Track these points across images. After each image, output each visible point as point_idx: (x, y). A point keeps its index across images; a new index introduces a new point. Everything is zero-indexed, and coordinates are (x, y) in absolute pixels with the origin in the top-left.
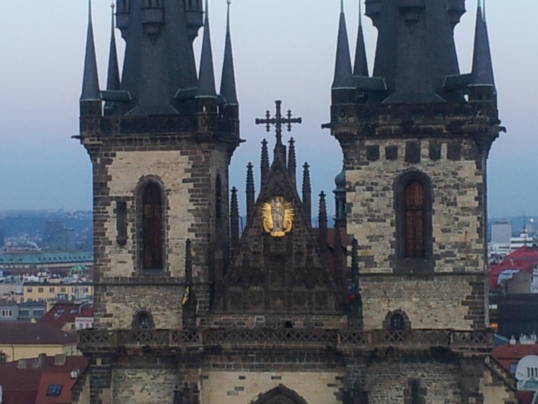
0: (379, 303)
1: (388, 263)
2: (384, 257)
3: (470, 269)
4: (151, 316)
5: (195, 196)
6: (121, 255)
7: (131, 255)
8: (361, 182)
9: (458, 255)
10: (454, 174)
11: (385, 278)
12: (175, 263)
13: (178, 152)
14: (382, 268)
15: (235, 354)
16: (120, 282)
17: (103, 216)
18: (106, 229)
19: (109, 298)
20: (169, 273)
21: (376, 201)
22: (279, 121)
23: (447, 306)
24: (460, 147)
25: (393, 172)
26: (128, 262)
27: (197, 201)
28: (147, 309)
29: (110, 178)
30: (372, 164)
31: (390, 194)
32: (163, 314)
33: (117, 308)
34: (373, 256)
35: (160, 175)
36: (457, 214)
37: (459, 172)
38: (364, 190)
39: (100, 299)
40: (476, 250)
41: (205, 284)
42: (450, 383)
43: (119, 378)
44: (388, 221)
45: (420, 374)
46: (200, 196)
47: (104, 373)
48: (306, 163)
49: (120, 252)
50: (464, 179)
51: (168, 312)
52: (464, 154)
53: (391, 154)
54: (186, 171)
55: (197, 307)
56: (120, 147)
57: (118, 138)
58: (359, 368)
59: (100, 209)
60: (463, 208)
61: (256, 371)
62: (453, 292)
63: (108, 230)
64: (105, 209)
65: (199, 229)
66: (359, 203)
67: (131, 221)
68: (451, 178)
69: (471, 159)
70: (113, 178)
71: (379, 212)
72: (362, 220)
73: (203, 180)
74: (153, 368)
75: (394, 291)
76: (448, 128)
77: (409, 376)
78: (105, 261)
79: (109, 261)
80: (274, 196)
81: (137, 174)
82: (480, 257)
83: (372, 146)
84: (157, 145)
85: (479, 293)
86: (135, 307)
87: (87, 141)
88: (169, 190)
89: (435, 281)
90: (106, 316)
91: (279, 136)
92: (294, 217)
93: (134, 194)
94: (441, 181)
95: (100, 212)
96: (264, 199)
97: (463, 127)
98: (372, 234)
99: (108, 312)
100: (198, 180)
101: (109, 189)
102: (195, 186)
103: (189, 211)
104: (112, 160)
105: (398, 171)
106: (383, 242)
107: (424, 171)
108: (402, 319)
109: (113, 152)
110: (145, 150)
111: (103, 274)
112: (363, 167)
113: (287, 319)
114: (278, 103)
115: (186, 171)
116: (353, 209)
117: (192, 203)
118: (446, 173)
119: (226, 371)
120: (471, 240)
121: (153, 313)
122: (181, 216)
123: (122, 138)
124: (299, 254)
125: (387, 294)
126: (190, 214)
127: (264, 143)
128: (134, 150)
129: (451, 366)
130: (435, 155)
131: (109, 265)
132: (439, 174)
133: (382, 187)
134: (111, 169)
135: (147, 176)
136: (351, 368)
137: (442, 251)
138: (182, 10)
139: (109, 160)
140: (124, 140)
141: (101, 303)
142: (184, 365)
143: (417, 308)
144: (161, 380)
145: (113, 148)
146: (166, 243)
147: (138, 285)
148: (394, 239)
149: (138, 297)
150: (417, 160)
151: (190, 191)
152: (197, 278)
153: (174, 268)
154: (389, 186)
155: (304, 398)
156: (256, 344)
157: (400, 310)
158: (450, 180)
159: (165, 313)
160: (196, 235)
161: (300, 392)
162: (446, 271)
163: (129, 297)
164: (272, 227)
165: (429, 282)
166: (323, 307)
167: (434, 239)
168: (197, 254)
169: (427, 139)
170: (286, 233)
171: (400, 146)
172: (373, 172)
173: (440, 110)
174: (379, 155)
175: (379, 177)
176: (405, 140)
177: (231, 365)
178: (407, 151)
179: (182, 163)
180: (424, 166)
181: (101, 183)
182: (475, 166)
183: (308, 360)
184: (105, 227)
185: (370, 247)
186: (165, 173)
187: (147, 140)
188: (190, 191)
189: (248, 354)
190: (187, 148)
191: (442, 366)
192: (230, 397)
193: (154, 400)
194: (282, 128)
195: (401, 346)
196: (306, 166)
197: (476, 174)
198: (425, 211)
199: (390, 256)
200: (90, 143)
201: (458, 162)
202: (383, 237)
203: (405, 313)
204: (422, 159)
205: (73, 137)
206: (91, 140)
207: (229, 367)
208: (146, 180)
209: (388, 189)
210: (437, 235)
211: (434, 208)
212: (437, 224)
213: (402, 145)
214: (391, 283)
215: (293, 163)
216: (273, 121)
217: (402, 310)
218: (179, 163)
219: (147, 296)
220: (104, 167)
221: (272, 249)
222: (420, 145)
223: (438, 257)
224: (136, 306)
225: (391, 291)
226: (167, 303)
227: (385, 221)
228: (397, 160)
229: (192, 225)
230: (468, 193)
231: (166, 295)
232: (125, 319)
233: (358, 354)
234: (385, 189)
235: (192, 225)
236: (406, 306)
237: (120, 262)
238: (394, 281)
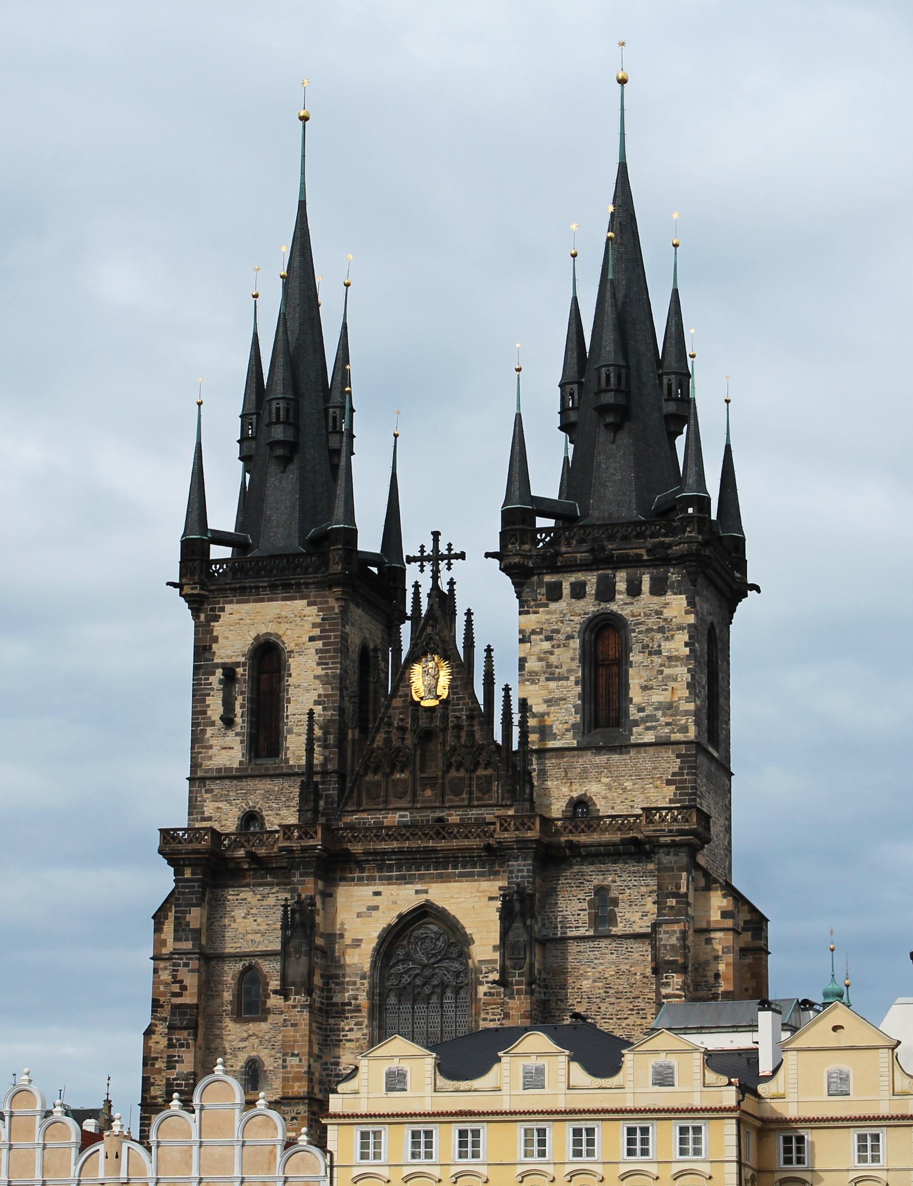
0: (557, 787)
1: (571, 734)
2: (566, 726)
3: (678, 737)
4: (262, 818)
5: (325, 658)
9: (662, 719)
10: (659, 613)
11: (567, 753)
12: (295, 746)
13: (305, 602)
15: (368, 861)
16: (225, 775)
18: (209, 706)
19: (209, 795)
20: (287, 760)
21: (556, 653)
22: (436, 558)
23: (647, 786)
24: (667, 578)
25: (580, 615)
27: (327, 664)
28: (257, 809)
29: (215, 640)
30: (553, 606)
31: (576, 643)
34: (551, 726)
35: (280, 633)
36: (661, 665)
37: (665, 611)
38: (541, 640)
39: (196, 797)
40: (686, 711)
41: (333, 772)
42: (649, 889)
43: (216, 900)
44: (572, 678)
45: (610, 879)
46: (330, 658)
47: (193, 887)
48: (469, 610)
49: (225, 735)
50: (671, 620)
51: (284, 812)
52: (672, 587)
53: (578, 592)
55: (322, 803)
57: (228, 586)
58: (524, 866)
59: (201, 679)
60: (670, 658)
61: (396, 884)
62: (655, 769)
64: (208, 679)
65: (328, 700)
66: (535, 658)
68: (653, 619)
69: (681, 594)
72: (538, 680)
73: (335, 637)
74: (260, 885)
75: (579, 770)
76: (649, 552)
77: (596, 882)
79: (211, 747)
80: (425, 655)
82: (690, 720)
85: (690, 768)
87: (187, 590)
88: (292, 652)
89: (632, 754)
90: (204, 819)
91: (435, 577)
92: (452, 680)
94: (641, 623)
95: (201, 684)
96: (414, 658)
97: (670, 551)
99: (207, 814)
100: (329, 637)
101: (214, 653)
102: (324, 645)
103: (316, 677)
104: (220, 616)
105: (585, 614)
106: (565, 706)
108: (587, 807)
110: (262, 600)
113: (438, 814)
114: (436, 535)
115: (315, 625)
117: (320, 667)
118: (648, 613)
119: (356, 885)
120: (680, 699)
121: (264, 813)
123: (233, 586)
124: (458, 728)
126: (318, 682)
128: (248, 602)
129: (651, 866)
130: (634, 590)
131: (211, 752)
132: (640, 615)
133: (564, 636)
134: (218, 628)
136: (514, 865)
137: (641, 714)
138: (324, 431)
142: (298, 873)
144: (271, 900)
145: (221, 600)
147: (246, 777)
148: (580, 702)
149: (246, 793)
150: (612, 599)
151: (318, 651)
153: (294, 754)
155: (457, 917)
156: (395, 845)
157: (585, 795)
158: (652, 622)
160: (324, 709)
161: (452, 910)
162: (646, 741)
164: (423, 695)
165: (624, 757)
166: (486, 797)
167: (631, 699)
169: (625, 570)
170: (442, 702)
171: (590, 580)
173: (637, 530)
174: (562, 594)
175: (562, 622)
177: (363, 877)
178: (598, 586)
179: (309, 616)
180: (620, 605)
182: (685, 603)
183: (464, 867)
184: (207, 702)
185: (548, 714)
187: (264, 587)
188: (318, 651)
189: (385, 860)
190: (316, 597)
191: (639, 867)
192: (359, 919)
193: (259, 928)
194: (441, 567)
195: (583, 839)
196: (469, 613)
197: (687, 612)
198: (621, 664)
199: (573, 725)
200: (190, 592)
201: (663, 598)
202: (565, 699)
203: (591, 799)
204: (617, 597)
205: (168, 584)
206: (193, 589)
207: (361, 879)
210: (636, 695)
211: (631, 659)
212: (635, 679)
213: (591, 580)
216: (428, 558)
220: (210, 626)
221: (423, 723)
222: (614, 577)
223: (636, 723)
226: (284, 799)
227: (568, 679)
229: (319, 696)
230: (676, 637)
231: (283, 789)
232: (229, 823)
233: (523, 843)
234: (569, 637)
235: (319, 696)
236: (594, 789)
237: (225, 748)
238: (578, 757)
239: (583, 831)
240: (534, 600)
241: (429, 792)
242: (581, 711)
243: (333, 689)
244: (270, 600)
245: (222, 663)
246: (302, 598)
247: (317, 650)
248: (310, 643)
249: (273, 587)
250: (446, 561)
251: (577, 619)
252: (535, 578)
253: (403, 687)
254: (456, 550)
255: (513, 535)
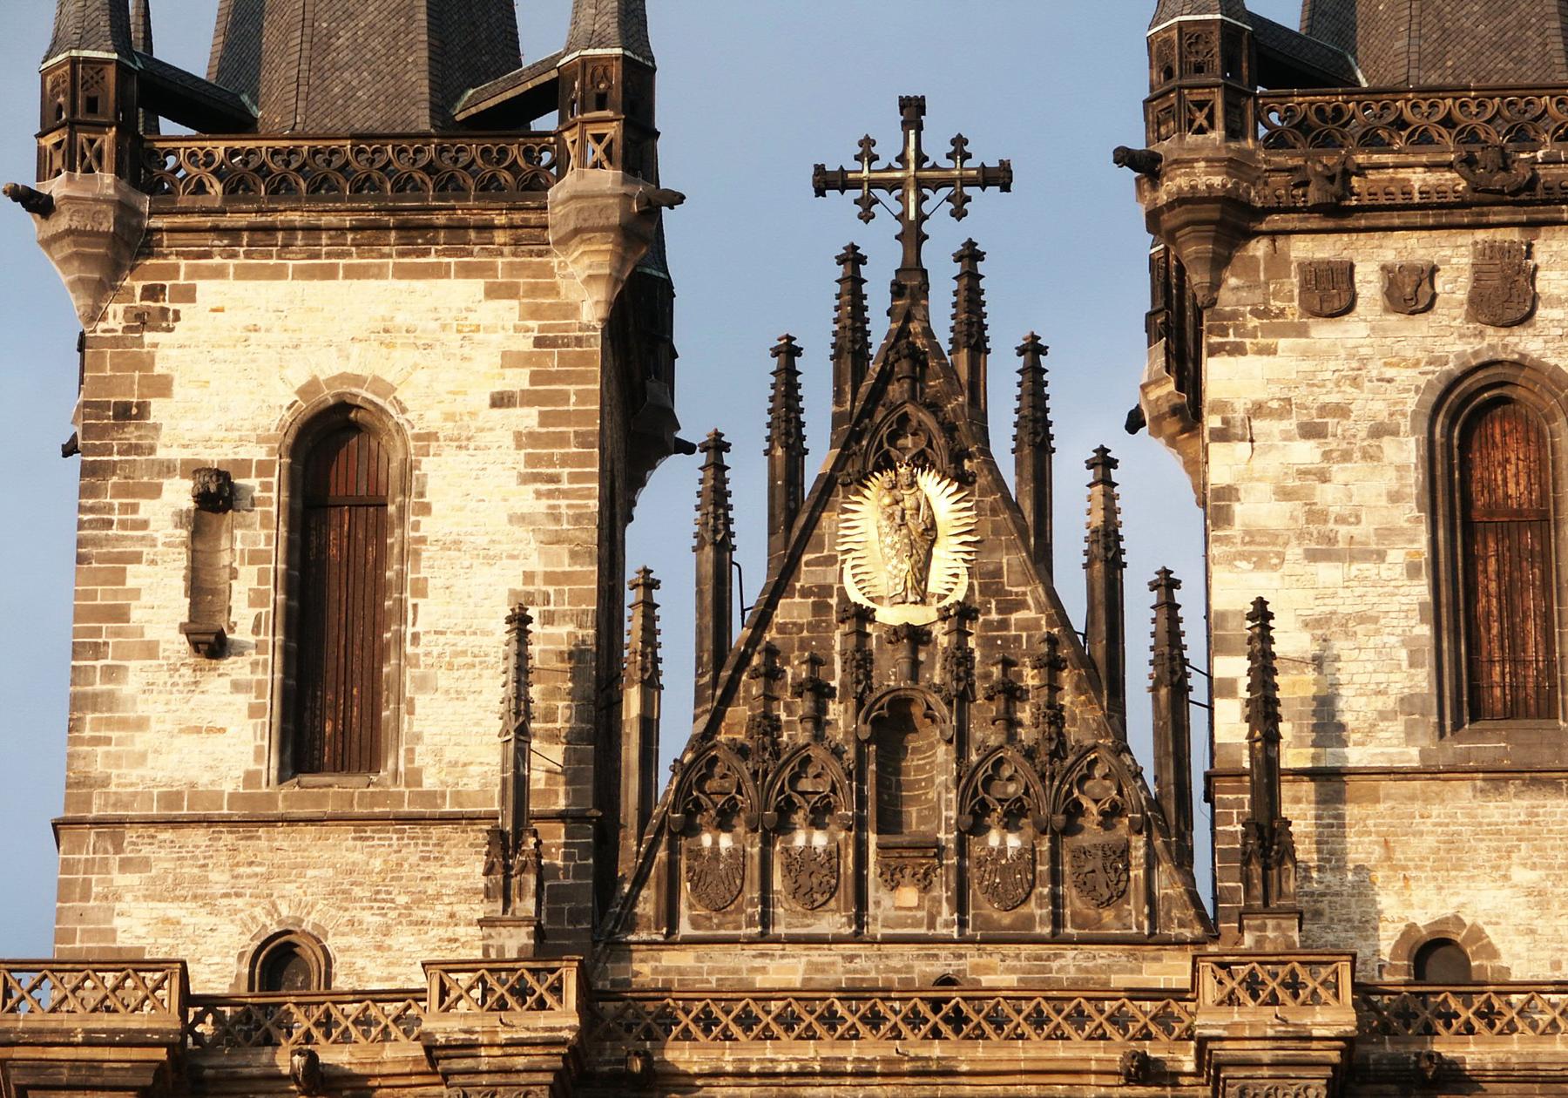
1: (1397, 727)
2: (1379, 703)
6: (197, 697)
7: (244, 700)
8: (1275, 404)
11: (1386, 785)
13: (477, 285)
14: (1372, 749)
17: (119, 539)
18: (136, 593)
20: (415, 777)
25: (1417, 364)
26: (230, 730)
27: (553, 479)
28: (307, 926)
29: (163, 387)
30: (1325, 333)
31: (1406, 451)
32: (379, 948)
33: (167, 921)
35: (389, 378)
38: (1287, 437)
39: (87, 882)
44: (1397, 556)
46: (565, 461)
53: (1411, 293)
54: (510, 359)
56: (217, 260)
57: (208, 221)
59: (111, 509)
63: (145, 598)
64: (134, 508)
65: (559, 593)
66: (1266, 488)
67: (252, 562)
70: (176, 388)
71: (1358, 522)
72: (1281, 557)
73: (583, 397)
75: (1430, 841)
78: (124, 724)
79: (141, 724)
81: (288, 373)
83: (1321, 262)
84: (382, 256)
86: (253, 918)
88: (431, 436)
91: (913, 236)
93: (271, 452)
95: (110, 524)
96: (847, 477)
98: (1320, 610)
101: (156, 428)
102: (545, 419)
105: (1430, 363)
106: (1376, 641)
107: (1553, 361)
109: (181, 281)
110: (329, 273)
111: (105, 782)
112: (1283, 343)
113: (944, 962)
114: (913, 111)
115: (510, 359)
116: (1237, 507)
121: (331, 943)
122: (483, 541)
123: (227, 221)
125: (1398, 855)
126: (520, 532)
127: (853, 258)
128: (278, 274)
131: (141, 741)
134: (166, 350)
135: (330, 382)
139: (164, 311)
140: (233, 233)
141: (92, 903)
143: (1535, 913)
145: (183, 263)
146: (409, 649)
149: (268, 877)
150: (1526, 319)
151: (524, 439)
152: (548, 793)
154: (1399, 417)
159: (388, 941)
163: (226, 877)
166: (1108, 915)
168: (551, 694)
172: (1332, 365)
175: (1355, 382)
176: (1466, 239)
181: (128, 406)
184: (131, 583)
186: (415, 366)
187: (342, 230)
188: (524, 439)
196: (1033, 349)
199: (1407, 703)
203: (1477, 934)
204: (1541, 312)
208: (328, 396)
209: (1395, 433)
213: (1454, 257)
214: (1417, 807)
215: (973, 335)
217: (1468, 921)
218: (478, 328)
219: (310, 873)
224: (258, 911)
225: (1414, 841)
227: (1381, 556)
228: (1430, 316)
229: (529, 577)
234: (1378, 431)
235: (529, 577)
237: (198, 730)
239: (1470, 1030)
240: (1256, 313)
241: (909, 895)
242: (1429, 658)
243: (574, 555)
244: (352, 273)
245: (185, 463)
246: (467, 272)
247: (518, 436)
248: (497, 412)
249: (370, 233)
250: (945, 192)
251: (1404, 375)
252: (1259, 248)
253: (807, 564)
254: (984, 154)
255: (1200, 105)
